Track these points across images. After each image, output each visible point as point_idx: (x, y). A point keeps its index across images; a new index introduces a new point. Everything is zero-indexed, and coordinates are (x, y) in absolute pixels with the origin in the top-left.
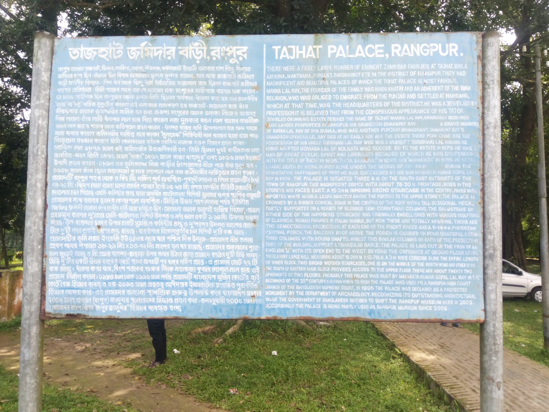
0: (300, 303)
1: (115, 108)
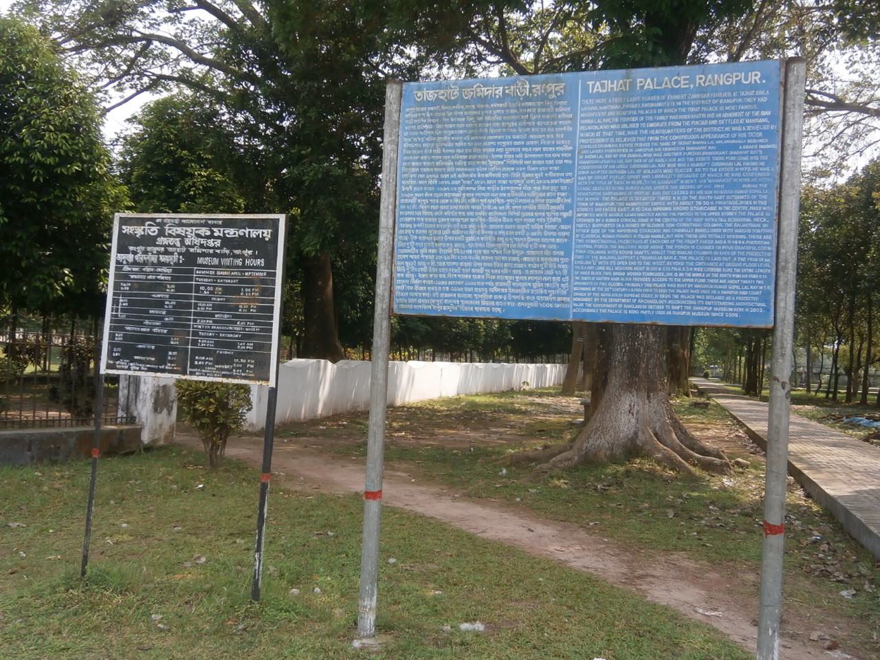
1: (452, 141)
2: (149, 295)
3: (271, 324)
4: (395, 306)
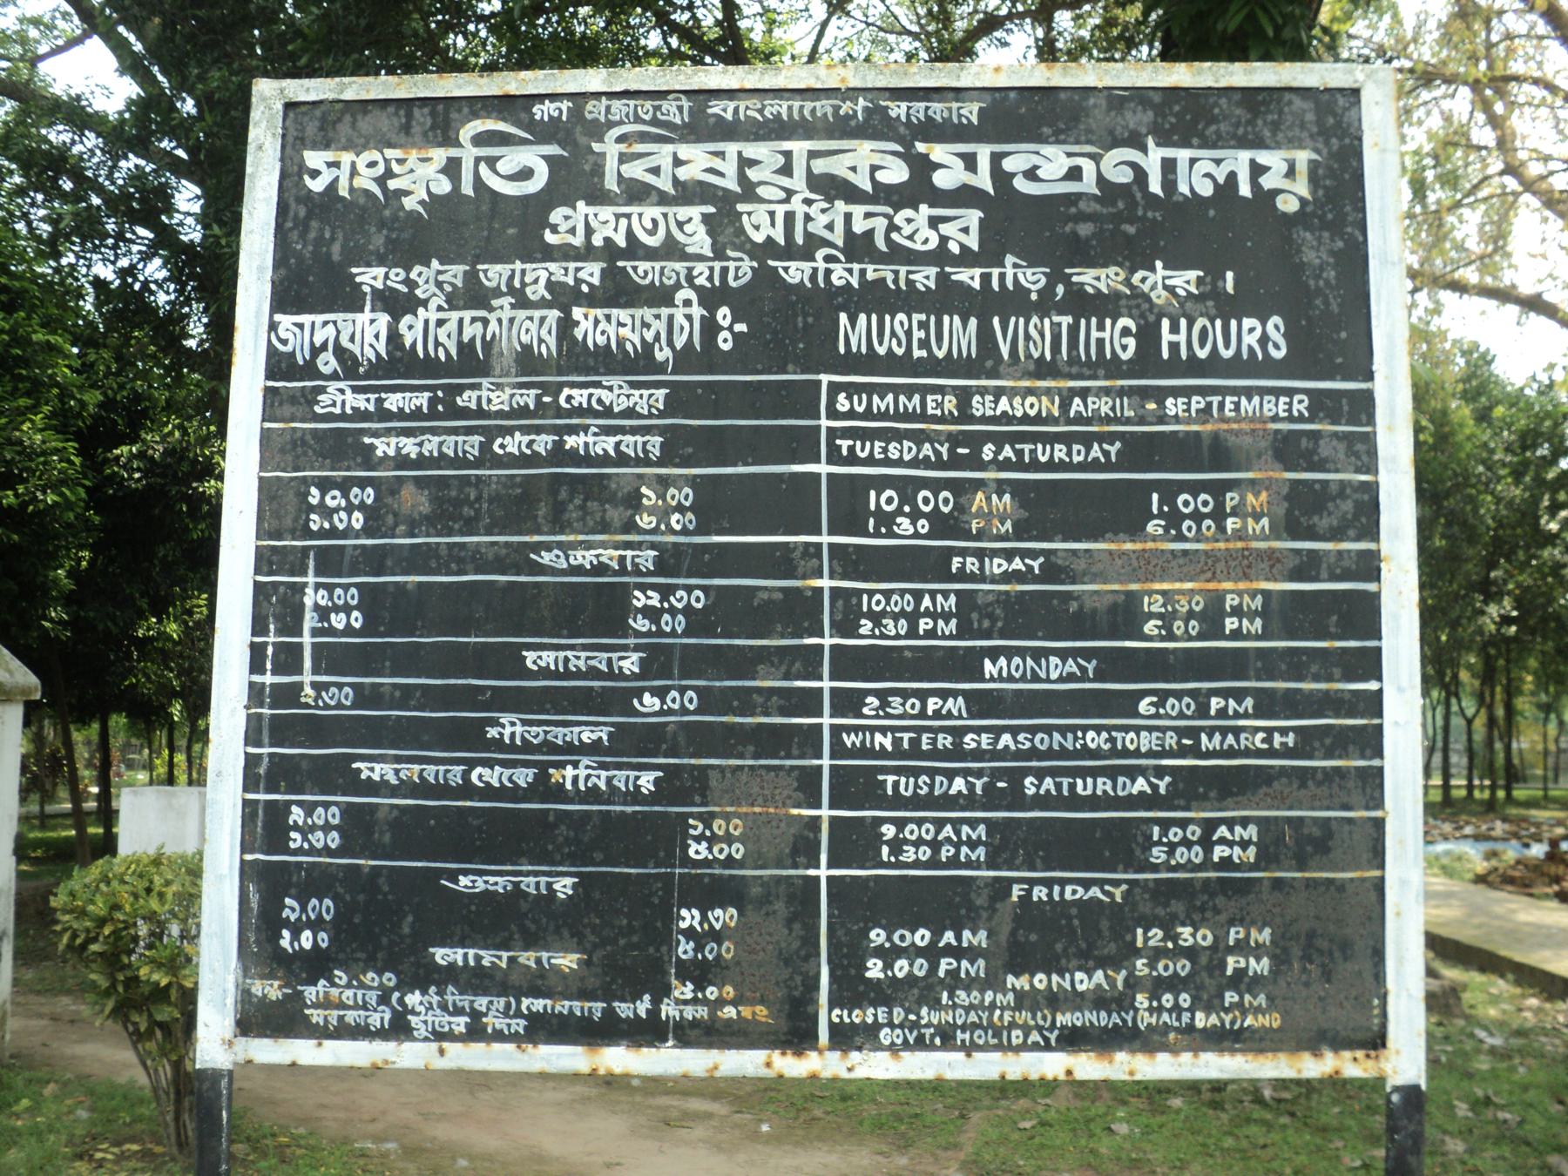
2: (519, 559)
3: (1374, 704)
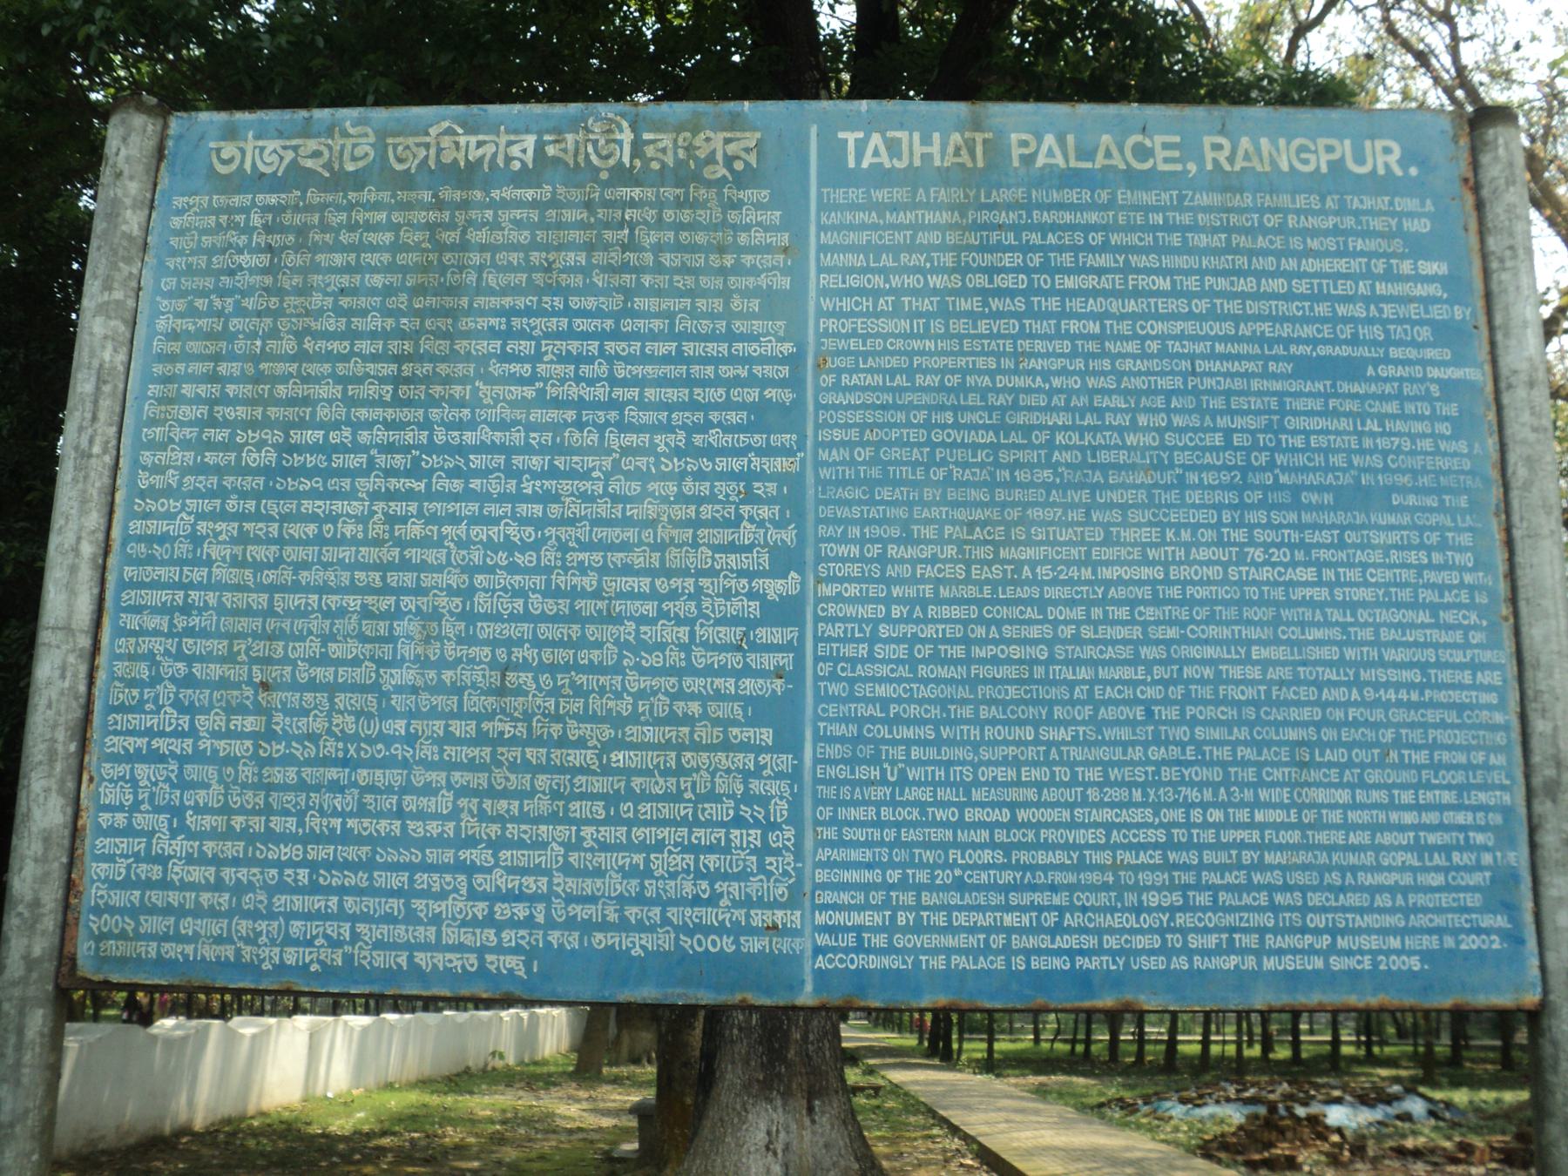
0: (935, 952)
1: (339, 312)
4: (84, 949)
